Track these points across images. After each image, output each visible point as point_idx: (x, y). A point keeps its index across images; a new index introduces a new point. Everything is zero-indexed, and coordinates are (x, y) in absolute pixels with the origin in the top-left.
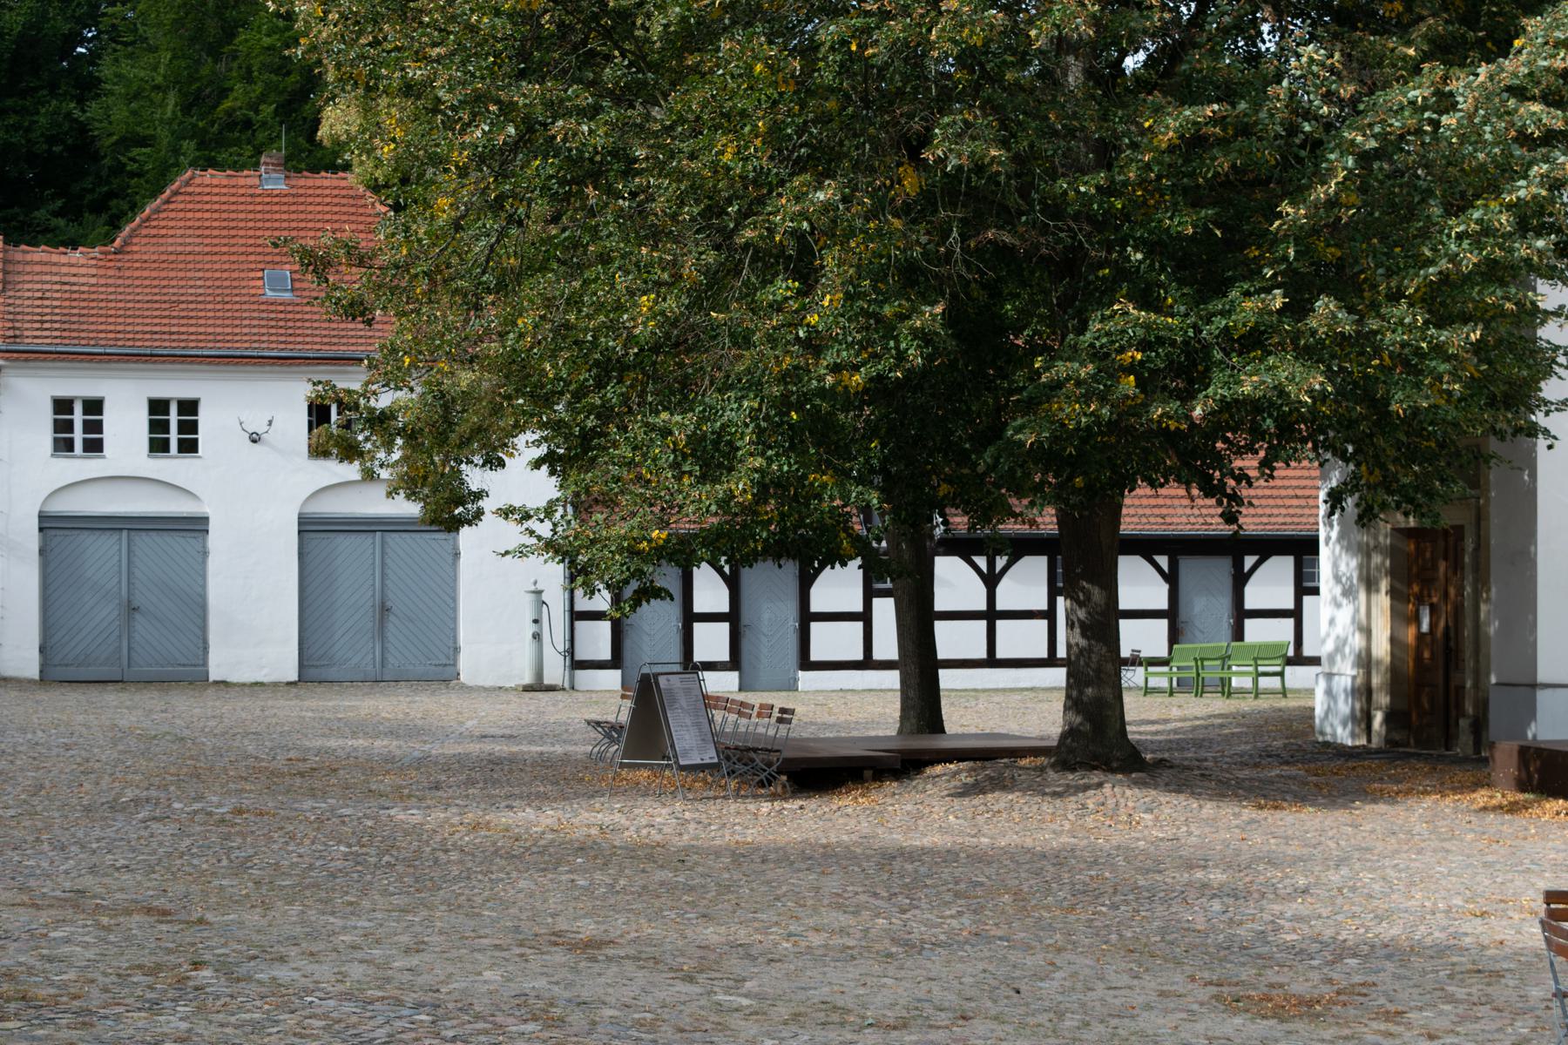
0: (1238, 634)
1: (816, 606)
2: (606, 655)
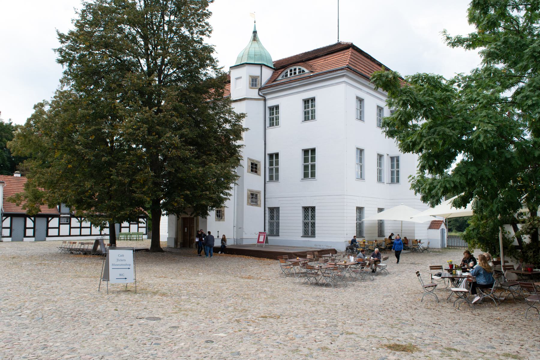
0: (120, 231)
1: (49, 226)
2: (9, 235)
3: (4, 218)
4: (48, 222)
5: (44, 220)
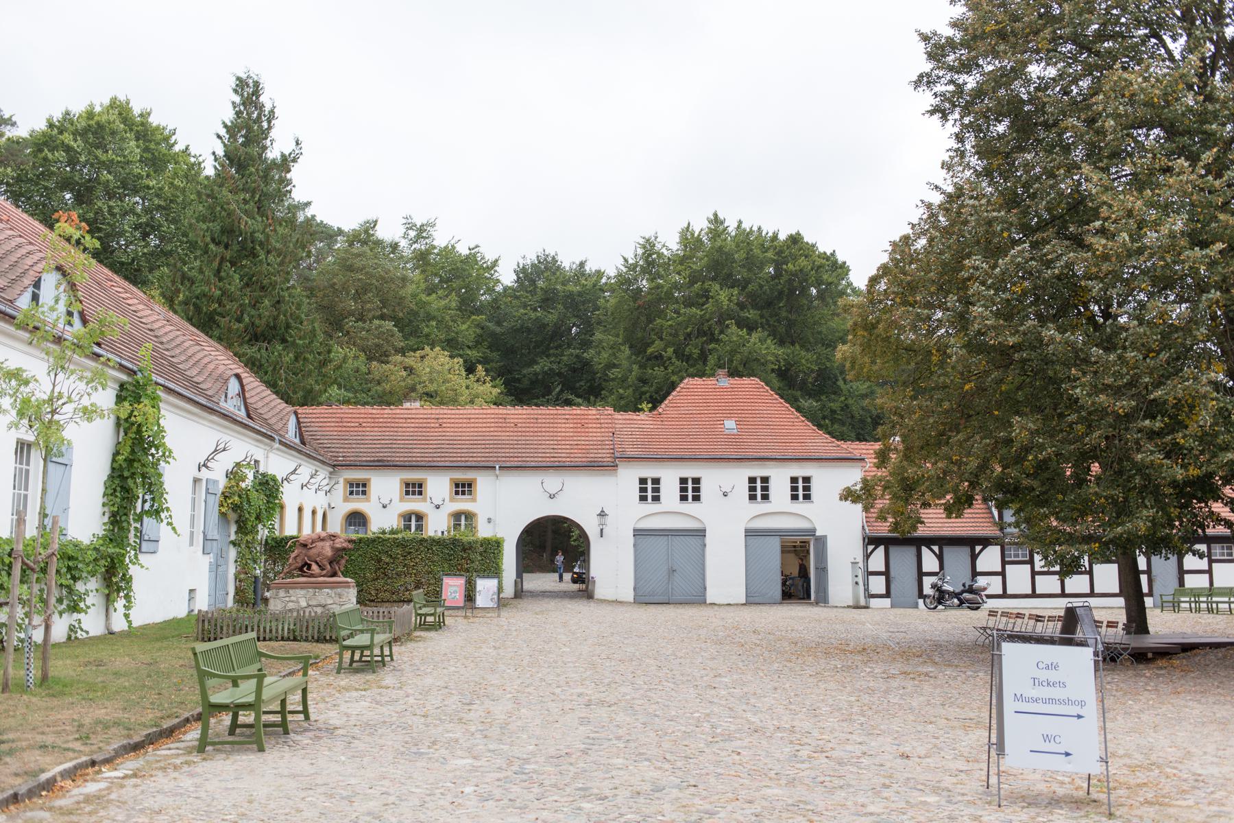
0: (1181, 583)
1: (979, 569)
2: (883, 591)
3: (870, 548)
4: (974, 557)
5: (963, 553)
